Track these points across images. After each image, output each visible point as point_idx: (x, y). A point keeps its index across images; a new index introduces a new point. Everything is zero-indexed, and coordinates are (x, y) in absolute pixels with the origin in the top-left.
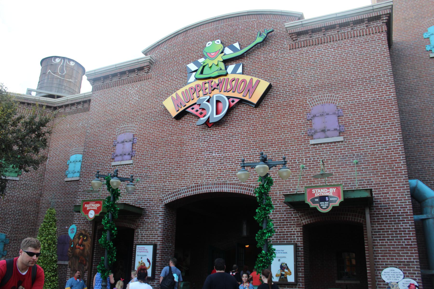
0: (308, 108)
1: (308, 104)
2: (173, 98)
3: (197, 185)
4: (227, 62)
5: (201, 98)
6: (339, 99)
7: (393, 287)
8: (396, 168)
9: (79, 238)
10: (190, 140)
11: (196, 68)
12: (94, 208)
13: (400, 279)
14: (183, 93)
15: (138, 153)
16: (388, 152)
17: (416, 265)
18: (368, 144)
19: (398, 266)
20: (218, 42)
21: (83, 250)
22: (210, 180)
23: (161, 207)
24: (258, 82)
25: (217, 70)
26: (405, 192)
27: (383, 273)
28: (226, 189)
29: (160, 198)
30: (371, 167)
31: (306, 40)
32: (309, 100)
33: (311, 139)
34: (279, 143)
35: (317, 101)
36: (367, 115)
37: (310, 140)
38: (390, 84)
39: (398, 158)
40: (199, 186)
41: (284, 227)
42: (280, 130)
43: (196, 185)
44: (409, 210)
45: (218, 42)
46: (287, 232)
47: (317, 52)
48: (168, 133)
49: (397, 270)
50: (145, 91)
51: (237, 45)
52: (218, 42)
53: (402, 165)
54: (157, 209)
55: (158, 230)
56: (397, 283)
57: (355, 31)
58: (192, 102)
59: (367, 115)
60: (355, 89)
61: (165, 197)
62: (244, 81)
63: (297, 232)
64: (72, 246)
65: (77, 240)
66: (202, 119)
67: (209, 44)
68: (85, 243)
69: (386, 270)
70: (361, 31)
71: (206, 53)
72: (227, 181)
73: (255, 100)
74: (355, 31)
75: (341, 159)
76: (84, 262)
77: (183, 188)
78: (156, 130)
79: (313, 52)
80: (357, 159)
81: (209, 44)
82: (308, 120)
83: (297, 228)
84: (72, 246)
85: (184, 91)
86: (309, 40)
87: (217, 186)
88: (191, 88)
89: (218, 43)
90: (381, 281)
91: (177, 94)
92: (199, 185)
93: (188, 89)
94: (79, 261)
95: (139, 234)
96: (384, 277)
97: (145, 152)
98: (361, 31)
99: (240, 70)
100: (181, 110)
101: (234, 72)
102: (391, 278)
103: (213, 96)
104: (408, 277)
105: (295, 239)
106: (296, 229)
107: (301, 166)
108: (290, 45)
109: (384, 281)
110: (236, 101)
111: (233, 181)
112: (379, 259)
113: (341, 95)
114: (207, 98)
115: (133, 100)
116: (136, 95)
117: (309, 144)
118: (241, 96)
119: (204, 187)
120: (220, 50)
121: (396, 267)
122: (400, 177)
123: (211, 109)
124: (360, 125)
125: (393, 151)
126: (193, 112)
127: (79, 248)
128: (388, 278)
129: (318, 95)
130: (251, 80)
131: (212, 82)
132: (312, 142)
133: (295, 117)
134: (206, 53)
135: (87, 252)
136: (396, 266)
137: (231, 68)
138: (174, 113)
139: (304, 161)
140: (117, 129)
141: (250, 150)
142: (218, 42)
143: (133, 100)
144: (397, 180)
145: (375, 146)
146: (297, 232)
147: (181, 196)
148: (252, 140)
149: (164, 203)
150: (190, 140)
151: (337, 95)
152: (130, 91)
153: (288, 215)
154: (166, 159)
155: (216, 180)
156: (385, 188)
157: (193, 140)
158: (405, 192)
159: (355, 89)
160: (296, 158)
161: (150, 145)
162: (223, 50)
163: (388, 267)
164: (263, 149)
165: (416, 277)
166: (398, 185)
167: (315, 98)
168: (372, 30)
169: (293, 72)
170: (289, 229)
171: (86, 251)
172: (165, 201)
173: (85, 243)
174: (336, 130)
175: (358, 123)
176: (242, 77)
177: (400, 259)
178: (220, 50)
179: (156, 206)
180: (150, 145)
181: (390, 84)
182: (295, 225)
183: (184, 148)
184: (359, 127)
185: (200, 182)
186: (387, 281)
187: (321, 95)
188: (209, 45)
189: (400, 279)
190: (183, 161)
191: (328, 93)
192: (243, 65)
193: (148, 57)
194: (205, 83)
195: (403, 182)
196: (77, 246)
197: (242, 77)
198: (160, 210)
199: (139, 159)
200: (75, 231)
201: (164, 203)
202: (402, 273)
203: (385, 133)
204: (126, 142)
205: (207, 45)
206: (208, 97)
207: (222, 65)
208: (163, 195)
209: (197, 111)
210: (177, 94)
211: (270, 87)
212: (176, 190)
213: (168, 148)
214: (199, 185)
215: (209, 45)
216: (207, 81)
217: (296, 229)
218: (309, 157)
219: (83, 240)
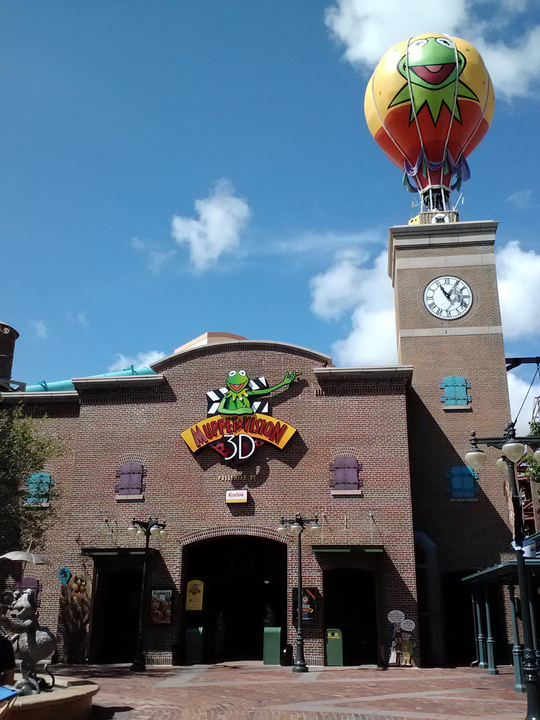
0: (331, 459)
1: (331, 455)
2: (192, 430)
3: (219, 527)
4: (252, 399)
5: (225, 436)
6: (359, 453)
7: (396, 627)
8: (404, 523)
10: (210, 478)
11: (218, 399)
13: (402, 620)
14: (204, 426)
15: (150, 487)
16: (398, 508)
17: (415, 608)
18: (383, 500)
19: (401, 609)
20: (242, 373)
22: (234, 523)
23: (178, 548)
24: (285, 427)
25: (242, 407)
26: (410, 546)
27: (389, 615)
28: (249, 533)
29: (178, 539)
30: (384, 521)
32: (332, 450)
33: (332, 489)
34: (303, 490)
35: (339, 453)
36: (383, 472)
37: (332, 491)
38: (405, 445)
39: (406, 515)
40: (222, 528)
41: (306, 572)
42: (303, 477)
43: (218, 526)
44: (413, 561)
45: (243, 373)
46: (308, 576)
47: (342, 402)
48: (185, 468)
49: (400, 612)
50: (156, 415)
51: (262, 380)
52: (242, 373)
53: (409, 521)
54: (174, 550)
55: (176, 574)
56: (400, 623)
57: (378, 386)
58: (215, 439)
59: (383, 472)
60: (374, 446)
61: (183, 538)
62: (271, 423)
63: (317, 576)
66: (226, 459)
67: (232, 374)
70: (384, 388)
71: (230, 383)
72: (251, 524)
73: (281, 445)
74: (378, 386)
75: (358, 511)
77: (204, 529)
78: (171, 463)
79: (338, 401)
80: (372, 513)
81: (232, 374)
82: (331, 471)
83: (318, 573)
85: (206, 425)
86: (335, 387)
87: (241, 528)
88: (213, 423)
89: (242, 375)
90: (387, 622)
91: (197, 427)
92: (222, 527)
93: (210, 423)
95: (153, 578)
96: (389, 619)
97: (158, 487)
98: (384, 388)
99: (266, 409)
100: (202, 445)
101: (259, 410)
102: (396, 619)
103: (238, 436)
104: (408, 618)
105: (316, 583)
106: (317, 574)
107: (323, 514)
108: (317, 390)
109: (390, 622)
110: (262, 443)
111: (257, 524)
112: (387, 603)
113: (361, 450)
114: (230, 437)
115: (140, 424)
116: (143, 418)
117: (330, 494)
118: (267, 439)
119: (227, 529)
120: (245, 383)
121: (400, 610)
122: (406, 532)
123: (238, 449)
124: (376, 481)
125: (403, 508)
126: (216, 448)
128: (393, 619)
129: (340, 447)
130: (278, 423)
131: (236, 419)
132: (334, 492)
133: (318, 466)
134: (230, 383)
137: (257, 405)
138: (195, 449)
139: (326, 510)
140: (120, 456)
141: (275, 494)
142: (243, 373)
143: (140, 424)
144: (404, 535)
145: (388, 502)
146: (317, 576)
147: (202, 537)
148: (276, 484)
149: (182, 544)
150: (210, 478)
151: (358, 450)
152: (135, 411)
153: (309, 561)
154: (183, 497)
155: (239, 522)
156: (394, 541)
157: (214, 478)
158: (410, 546)
159: (374, 446)
160: (318, 507)
161: (164, 479)
162: (249, 382)
163: (393, 610)
164: (287, 494)
165: (414, 618)
166: (405, 539)
167: (338, 449)
168: (394, 388)
169: (319, 419)
170: (310, 574)
172: (184, 542)
174: (355, 483)
175: (375, 479)
176: (268, 419)
177: (403, 603)
178: (245, 383)
179: (173, 548)
180: (164, 479)
181: (405, 445)
182: (315, 570)
183: (204, 486)
184: (376, 483)
185: (222, 523)
186: (392, 622)
187: (343, 448)
188: (233, 375)
189: (402, 620)
190: (203, 500)
191: (350, 446)
192: (269, 403)
193: (160, 376)
194: (229, 420)
195: (409, 537)
197: (268, 419)
198: (179, 551)
199: (150, 494)
201: (182, 544)
202: (404, 615)
203: (397, 491)
204: (134, 473)
205: (230, 375)
206: (233, 436)
207: (247, 402)
208: (181, 536)
209: (220, 448)
210: (197, 427)
211: (296, 433)
212: (196, 531)
213: (186, 484)
214: (222, 527)
215: (233, 375)
216: (231, 417)
217: (317, 574)
218: (331, 506)
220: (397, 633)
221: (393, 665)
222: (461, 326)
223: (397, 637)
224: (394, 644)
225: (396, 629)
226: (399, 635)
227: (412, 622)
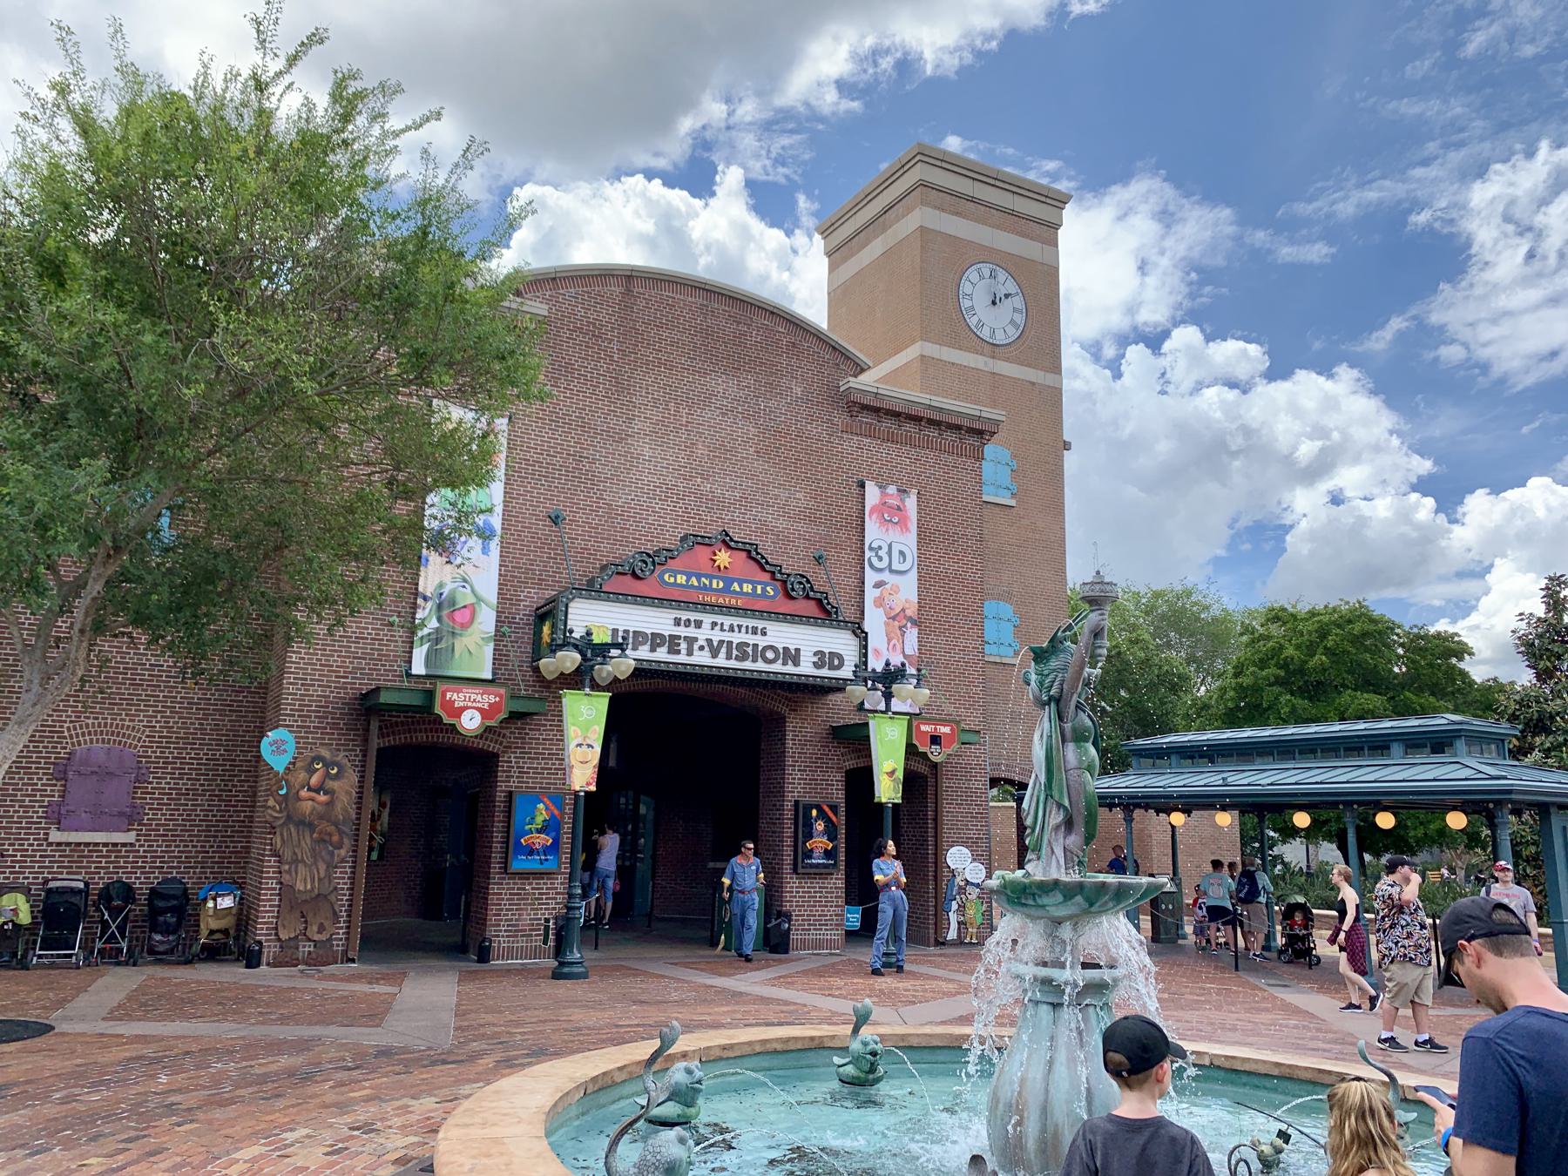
9: (313, 772)
12: (480, 705)
21: (330, 804)
31: (871, 424)
64: (283, 792)
65: (303, 775)
68: (330, 784)
69: (953, 850)
76: (335, 838)
84: (283, 792)
94: (315, 835)
104: (974, 860)
127: (312, 799)
135: (345, 810)
136: (963, 844)
171: (339, 807)
173: (330, 784)
196: (304, 793)
200: (291, 747)
219: (327, 775)
220: (960, 887)
221: (953, 944)
222: (1007, 360)
223: (959, 894)
224: (954, 906)
225: (959, 880)
226: (962, 890)
227: (981, 867)
